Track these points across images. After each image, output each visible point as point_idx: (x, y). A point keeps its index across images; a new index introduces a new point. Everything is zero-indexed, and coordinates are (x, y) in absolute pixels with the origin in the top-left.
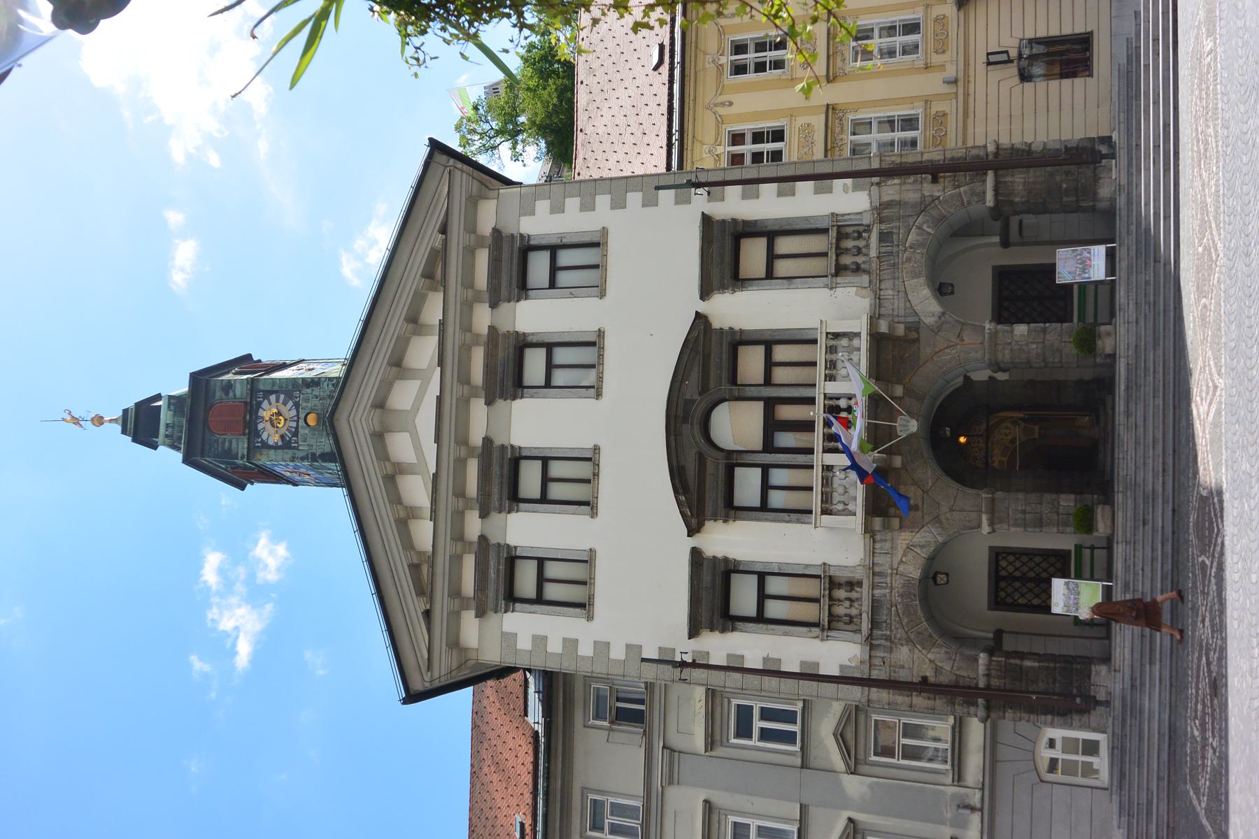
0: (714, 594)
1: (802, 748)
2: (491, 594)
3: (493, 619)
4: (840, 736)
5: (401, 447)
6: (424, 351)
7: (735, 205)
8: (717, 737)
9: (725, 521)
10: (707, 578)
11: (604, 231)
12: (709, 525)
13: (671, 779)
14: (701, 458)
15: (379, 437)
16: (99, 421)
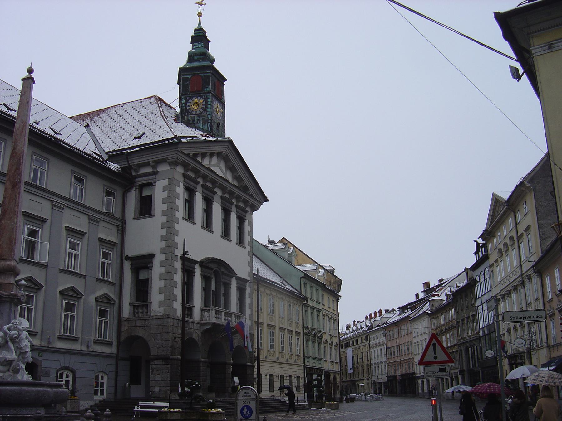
0: (188, 266)
1: (100, 279)
2: (188, 181)
3: (181, 179)
4: (106, 296)
5: (214, 160)
6: (229, 177)
7: (248, 290)
8: (103, 244)
9: (201, 275)
10: (192, 265)
11: (245, 247)
12: (200, 268)
13: (90, 218)
14: (211, 269)
15: (219, 154)
16: (200, 15)
